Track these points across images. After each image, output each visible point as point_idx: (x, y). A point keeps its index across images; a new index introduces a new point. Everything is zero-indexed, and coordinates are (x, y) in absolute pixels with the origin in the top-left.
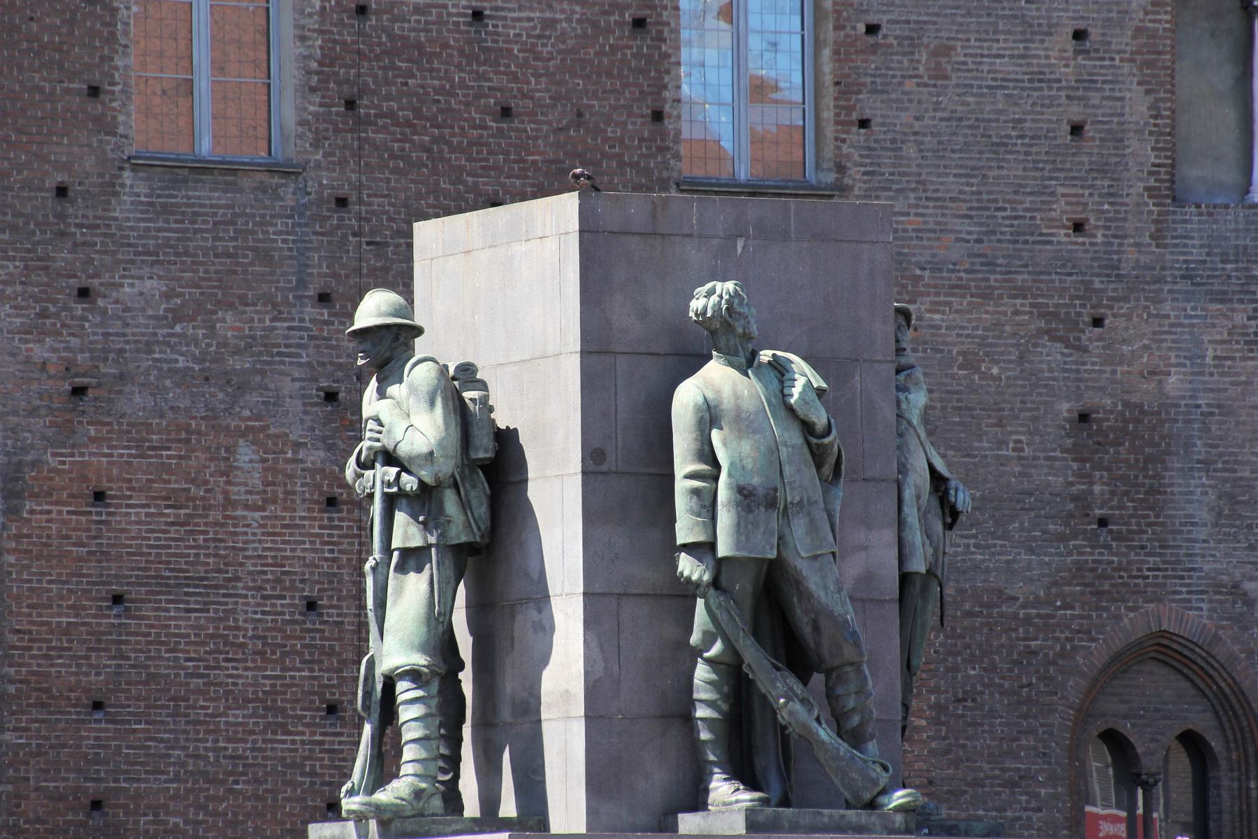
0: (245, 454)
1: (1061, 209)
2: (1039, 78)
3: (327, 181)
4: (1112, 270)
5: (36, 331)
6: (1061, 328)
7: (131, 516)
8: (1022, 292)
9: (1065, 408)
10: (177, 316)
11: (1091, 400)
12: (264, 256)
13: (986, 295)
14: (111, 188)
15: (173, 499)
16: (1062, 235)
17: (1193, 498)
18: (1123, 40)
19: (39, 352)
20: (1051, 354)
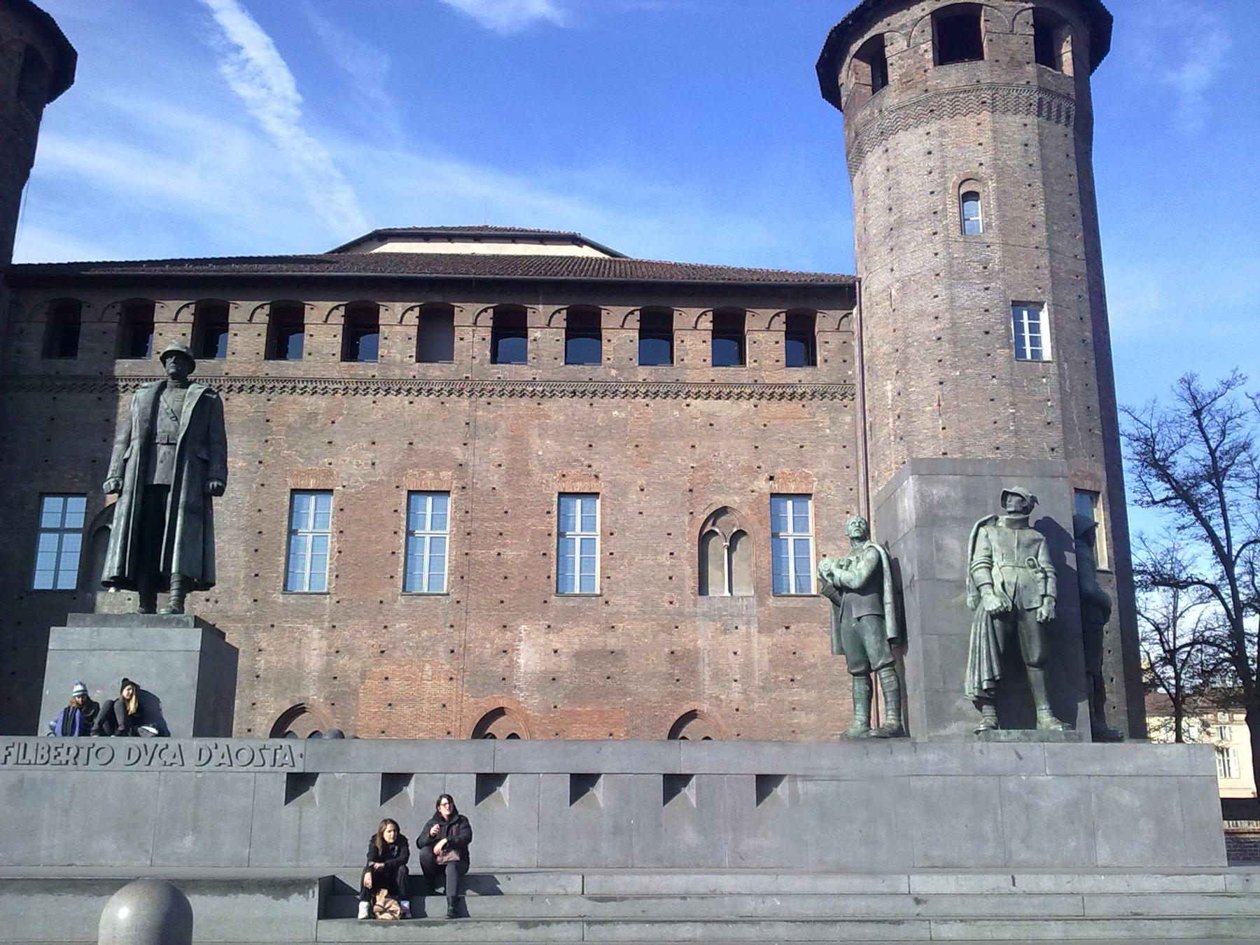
0: (428, 667)
1: (666, 598)
2: (660, 565)
3: (455, 597)
4: (681, 614)
5: (371, 637)
6: (665, 629)
7: (395, 683)
8: (654, 620)
9: (667, 650)
10: (410, 632)
11: (674, 648)
12: (435, 616)
13: (644, 621)
14: (395, 601)
15: (407, 679)
16: (667, 605)
17: (706, 673)
18: (684, 555)
19: (371, 642)
20: (663, 635)
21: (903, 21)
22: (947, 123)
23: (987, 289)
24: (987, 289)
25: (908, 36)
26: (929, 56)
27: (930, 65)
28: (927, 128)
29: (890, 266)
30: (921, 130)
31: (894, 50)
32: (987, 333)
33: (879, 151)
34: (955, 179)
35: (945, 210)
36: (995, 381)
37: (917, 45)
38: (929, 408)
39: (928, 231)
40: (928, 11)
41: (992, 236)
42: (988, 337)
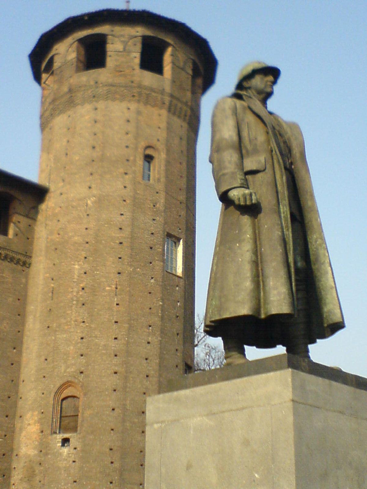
21: (122, 33)
22: (142, 107)
23: (154, 220)
24: (154, 220)
25: (125, 44)
26: (137, 61)
27: (137, 67)
28: (129, 105)
29: (88, 184)
30: (124, 105)
31: (113, 47)
32: (151, 248)
33: (88, 107)
34: (143, 144)
35: (135, 161)
36: (152, 281)
37: (130, 52)
38: (108, 288)
39: (122, 170)
40: (139, 34)
41: (160, 187)
42: (152, 251)
